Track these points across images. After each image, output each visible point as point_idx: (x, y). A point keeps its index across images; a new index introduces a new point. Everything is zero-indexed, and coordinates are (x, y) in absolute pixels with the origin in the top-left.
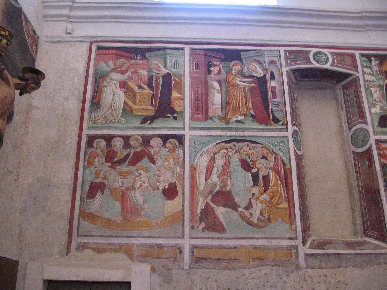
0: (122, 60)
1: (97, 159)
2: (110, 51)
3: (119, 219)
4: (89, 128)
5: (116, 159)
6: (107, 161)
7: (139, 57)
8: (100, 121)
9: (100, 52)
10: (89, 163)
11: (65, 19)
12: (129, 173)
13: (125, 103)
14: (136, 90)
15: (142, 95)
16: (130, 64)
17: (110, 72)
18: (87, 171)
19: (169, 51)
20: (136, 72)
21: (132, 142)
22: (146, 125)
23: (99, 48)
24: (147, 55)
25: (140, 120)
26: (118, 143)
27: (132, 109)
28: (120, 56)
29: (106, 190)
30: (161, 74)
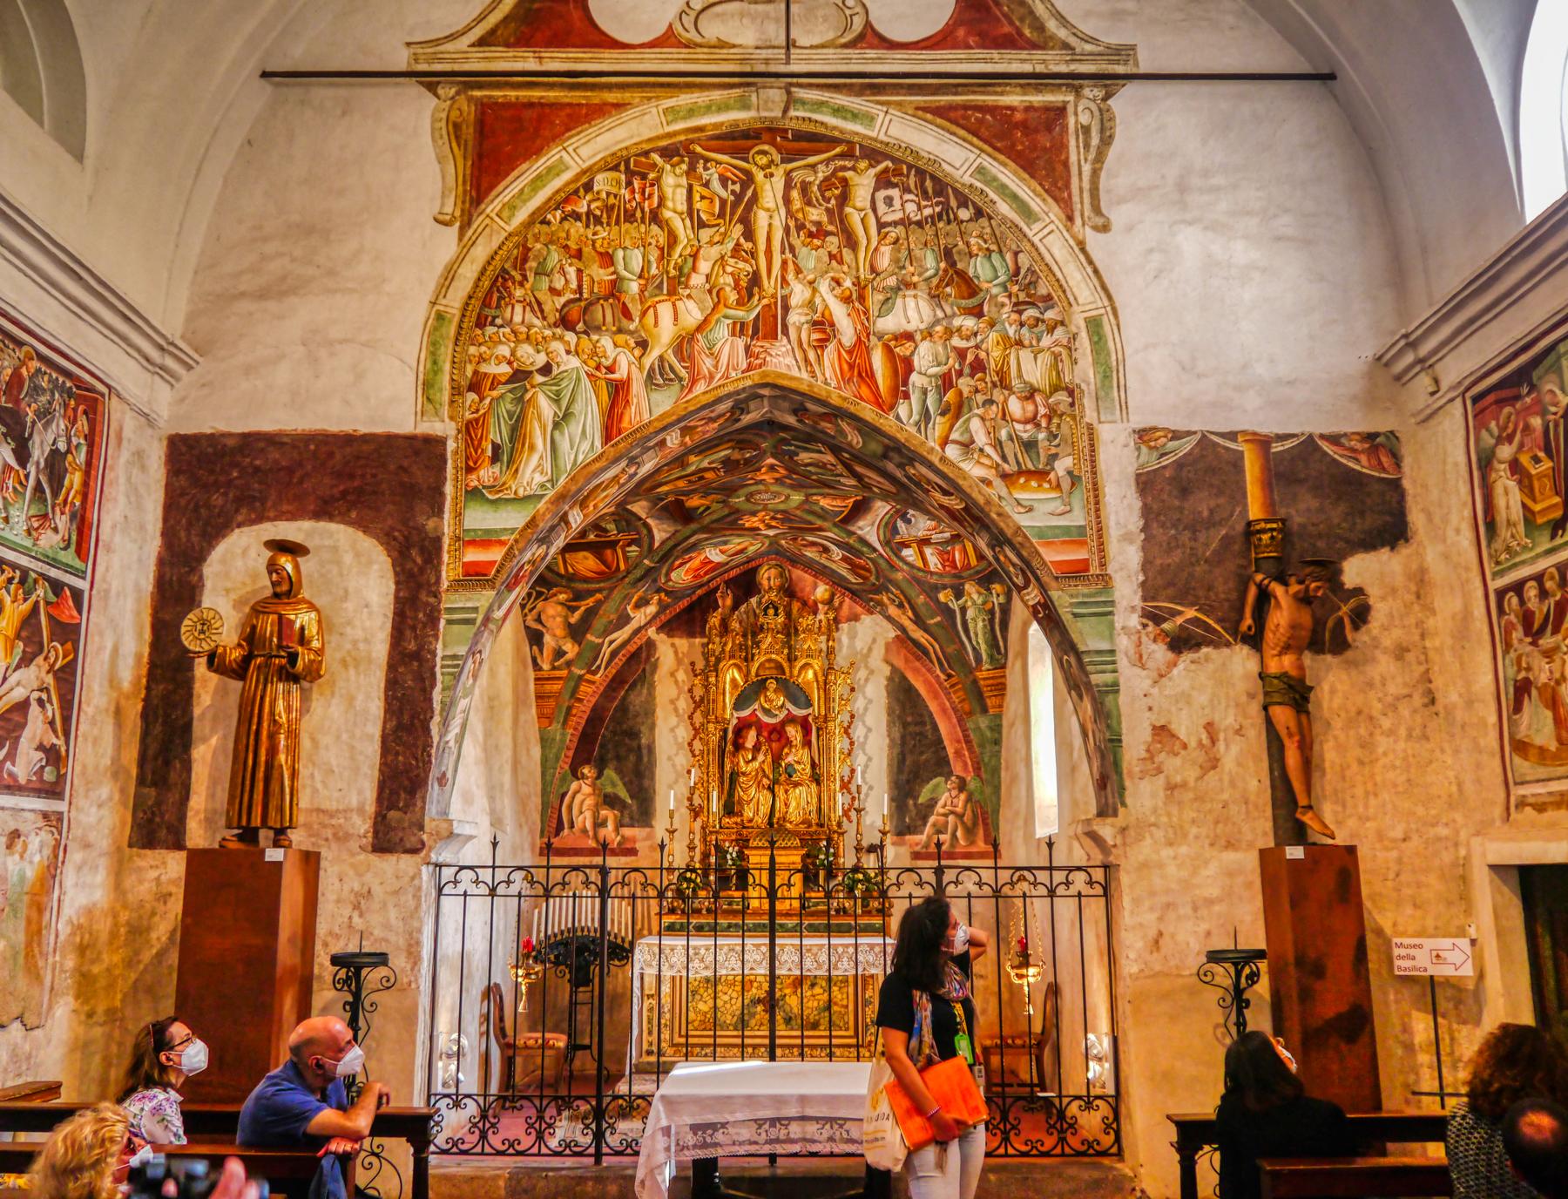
0: (1507, 410)
1: (1514, 635)
2: (1491, 398)
3: (1553, 746)
4: (1495, 575)
5: (1536, 626)
6: (1526, 635)
7: (1525, 390)
8: (1503, 557)
9: (1481, 405)
10: (1508, 646)
11: (1417, 368)
12: (1556, 649)
13: (1524, 505)
14: (1533, 472)
15: (1541, 476)
16: (1518, 413)
17: (1496, 445)
18: (1507, 661)
19: (1562, 348)
20: (1527, 429)
21: (1549, 585)
22: (1558, 541)
23: (1475, 400)
24: (1535, 375)
25: (1547, 533)
26: (1531, 591)
27: (1533, 513)
28: (1501, 403)
29: (1534, 692)
30: (1561, 413)
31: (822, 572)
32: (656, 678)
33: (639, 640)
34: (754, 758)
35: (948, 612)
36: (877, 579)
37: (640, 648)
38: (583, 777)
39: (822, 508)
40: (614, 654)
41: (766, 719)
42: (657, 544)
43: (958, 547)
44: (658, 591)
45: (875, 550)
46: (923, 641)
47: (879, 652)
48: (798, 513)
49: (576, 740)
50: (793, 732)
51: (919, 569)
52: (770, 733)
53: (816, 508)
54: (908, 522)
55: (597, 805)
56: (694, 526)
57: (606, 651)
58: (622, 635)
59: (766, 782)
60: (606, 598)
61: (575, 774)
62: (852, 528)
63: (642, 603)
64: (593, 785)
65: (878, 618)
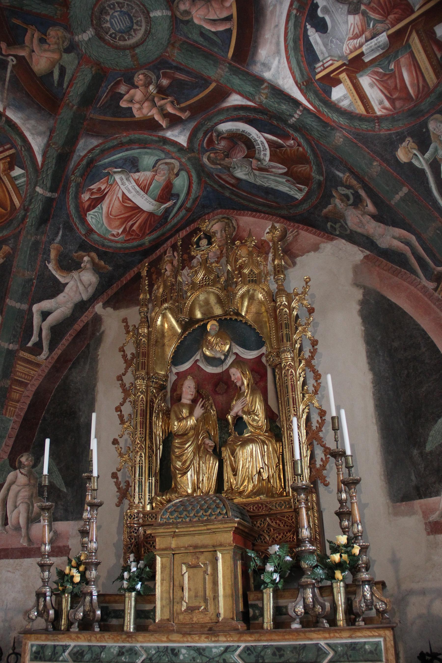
31: (268, 203)
32: (100, 351)
33: (85, 318)
34: (191, 413)
35: (414, 174)
36: (320, 173)
37: (87, 324)
38: (21, 466)
39: (202, 33)
40: (58, 331)
41: (210, 369)
42: (39, 159)
43: (404, 60)
44: (85, 247)
45: (296, 103)
46: (396, 244)
47: (346, 277)
48: (177, 56)
49: (17, 427)
50: (242, 378)
51: (360, 118)
52: (216, 385)
53: (195, 36)
54: (321, 27)
55: (31, 497)
56: (66, 114)
57: (42, 328)
58: (59, 306)
59: (210, 443)
60: (14, 249)
61: (14, 465)
62: (257, 69)
63: (70, 265)
64: (29, 475)
65: (342, 243)
